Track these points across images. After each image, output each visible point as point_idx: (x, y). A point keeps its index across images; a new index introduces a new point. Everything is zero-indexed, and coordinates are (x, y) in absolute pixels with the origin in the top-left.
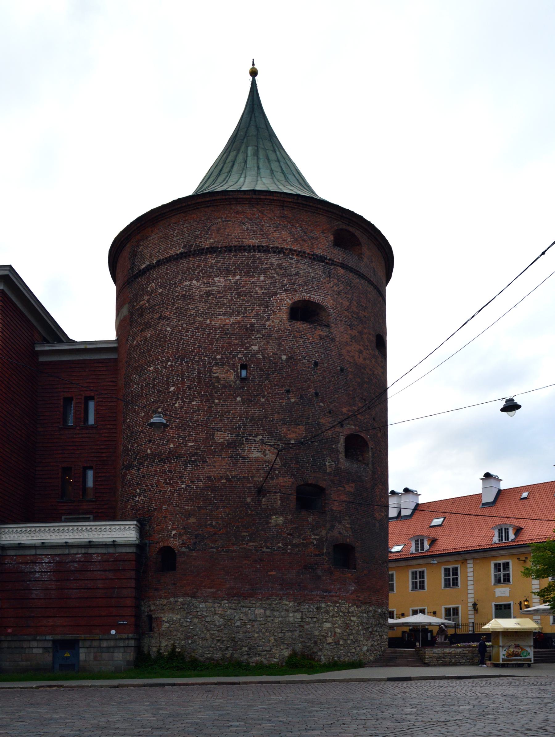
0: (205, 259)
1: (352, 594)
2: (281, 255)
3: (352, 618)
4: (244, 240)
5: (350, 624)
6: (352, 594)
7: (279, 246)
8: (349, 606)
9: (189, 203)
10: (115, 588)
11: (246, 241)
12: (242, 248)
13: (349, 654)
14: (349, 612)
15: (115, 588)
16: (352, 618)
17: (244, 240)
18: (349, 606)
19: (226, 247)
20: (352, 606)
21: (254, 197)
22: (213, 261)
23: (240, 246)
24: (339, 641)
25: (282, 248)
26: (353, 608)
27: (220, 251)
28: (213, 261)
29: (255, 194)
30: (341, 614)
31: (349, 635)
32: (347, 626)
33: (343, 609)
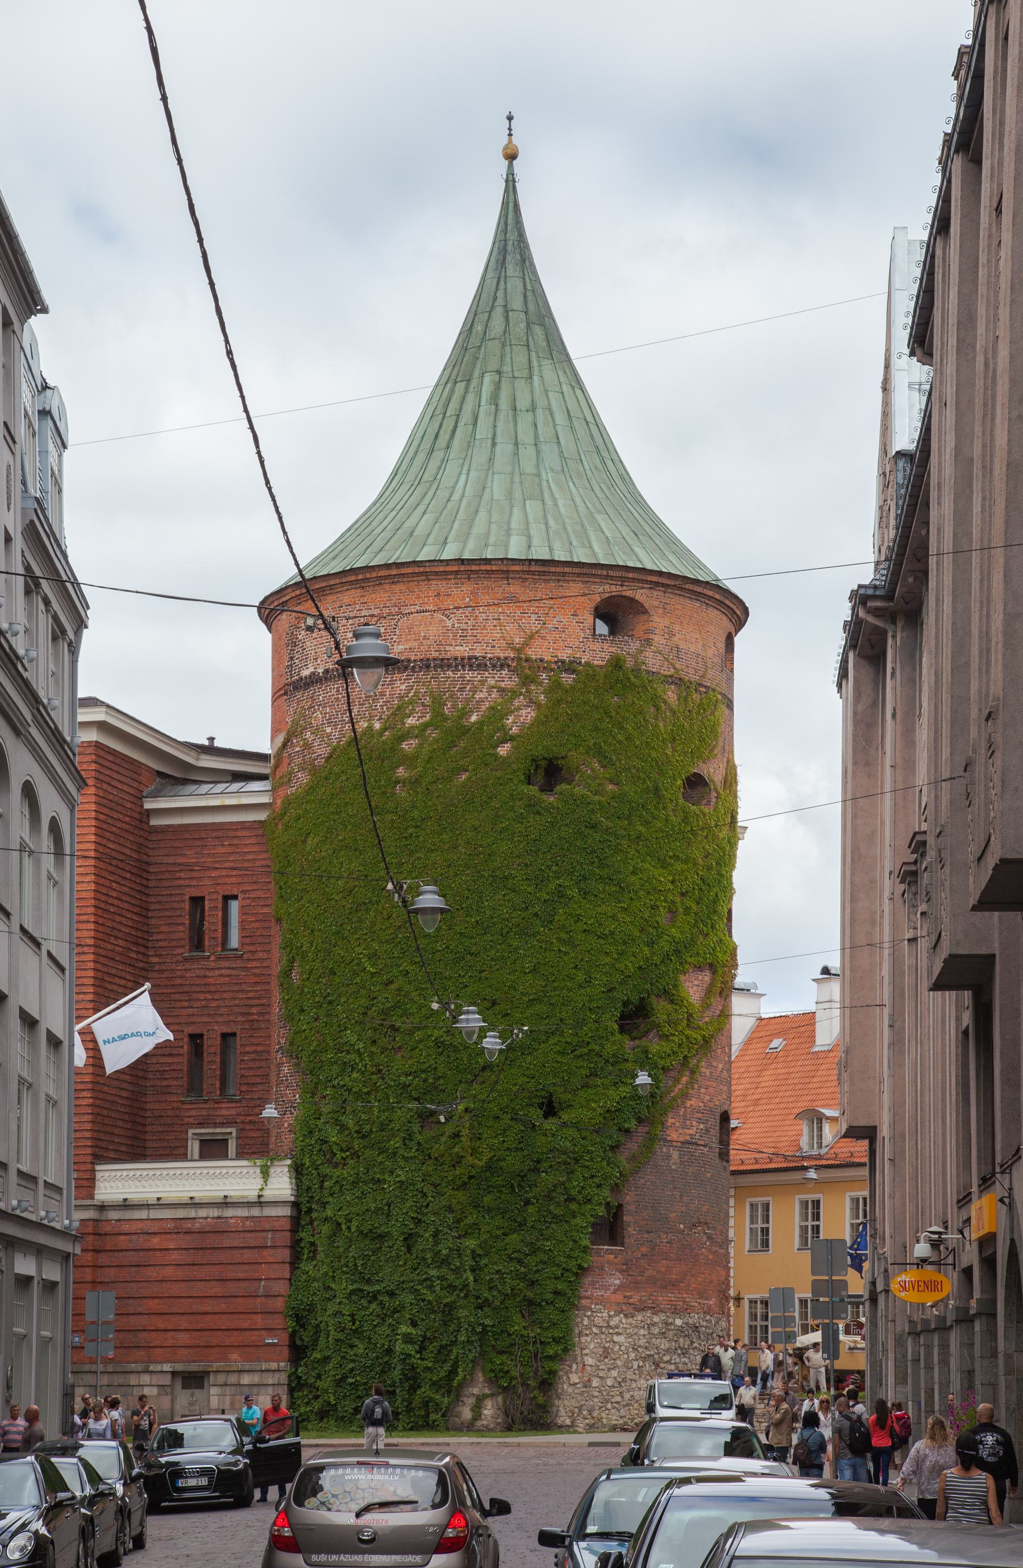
0: (392, 682)
1: (614, 1292)
2: (505, 672)
3: (616, 1338)
4: (448, 648)
5: (612, 1349)
6: (614, 1292)
7: (502, 655)
8: (610, 1316)
9: (368, 576)
10: (261, 1279)
11: (451, 648)
12: (445, 664)
13: (609, 1406)
14: (609, 1327)
15: (261, 1279)
16: (616, 1338)
17: (448, 648)
18: (610, 1316)
19: (421, 660)
20: (616, 1315)
21: (462, 568)
22: (403, 687)
23: (442, 660)
24: (589, 1380)
25: (506, 658)
26: (616, 1320)
27: (414, 667)
28: (403, 687)
29: (463, 564)
30: (594, 1330)
31: (609, 1370)
32: (606, 1353)
33: (598, 1321)
